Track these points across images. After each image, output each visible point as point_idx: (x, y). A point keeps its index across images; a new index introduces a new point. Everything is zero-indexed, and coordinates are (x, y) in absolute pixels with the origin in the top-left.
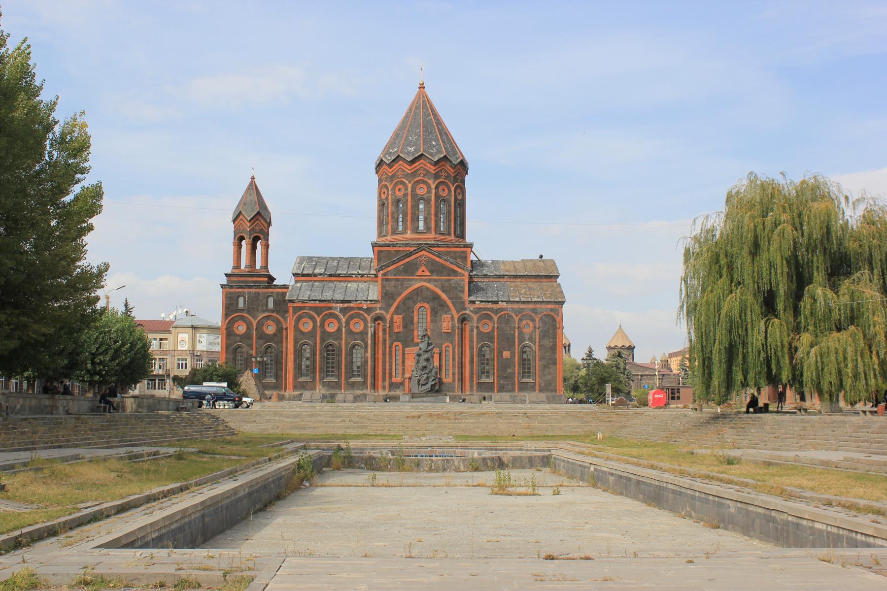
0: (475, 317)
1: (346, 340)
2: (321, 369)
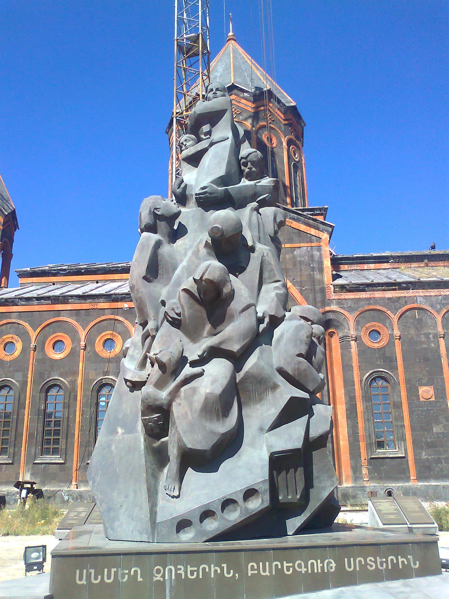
0: (351, 318)
1: (86, 375)
2: (31, 436)
